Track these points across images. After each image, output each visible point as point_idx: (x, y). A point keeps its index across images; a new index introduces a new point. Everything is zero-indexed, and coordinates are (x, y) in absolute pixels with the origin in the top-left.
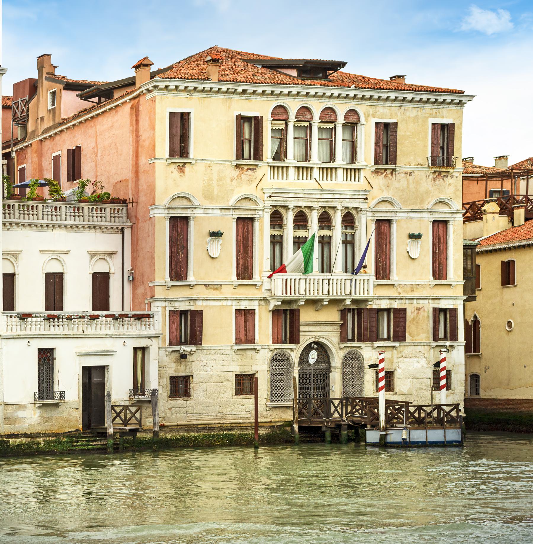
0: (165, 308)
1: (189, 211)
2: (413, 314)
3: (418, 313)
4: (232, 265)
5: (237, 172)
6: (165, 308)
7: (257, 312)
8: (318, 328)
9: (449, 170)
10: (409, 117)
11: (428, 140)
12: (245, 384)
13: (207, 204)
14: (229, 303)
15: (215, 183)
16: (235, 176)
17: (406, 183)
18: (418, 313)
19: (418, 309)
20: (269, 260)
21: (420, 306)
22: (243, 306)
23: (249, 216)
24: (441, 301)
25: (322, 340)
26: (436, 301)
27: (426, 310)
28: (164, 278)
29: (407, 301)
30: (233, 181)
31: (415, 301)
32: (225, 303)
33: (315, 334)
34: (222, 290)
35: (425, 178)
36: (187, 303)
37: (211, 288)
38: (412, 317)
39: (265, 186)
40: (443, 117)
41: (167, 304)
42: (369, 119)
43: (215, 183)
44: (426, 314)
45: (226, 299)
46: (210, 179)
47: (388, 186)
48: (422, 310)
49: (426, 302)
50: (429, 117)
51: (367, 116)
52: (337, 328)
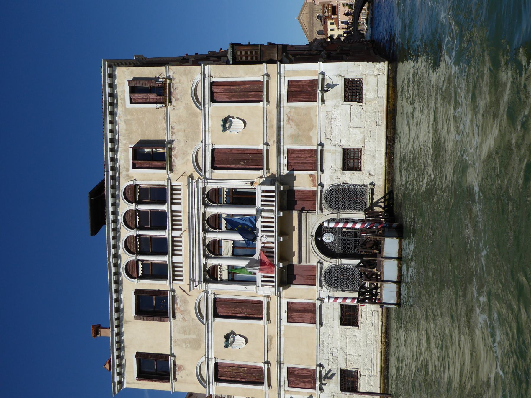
0: (285, 391)
1: (210, 363)
2: (293, 126)
3: (292, 120)
4: (251, 324)
5: (178, 315)
6: (285, 391)
7: (289, 300)
10: (126, 130)
11: (144, 108)
12: (353, 91)
13: (204, 345)
14: (282, 328)
15: (188, 337)
16: (182, 316)
17: (180, 133)
18: (292, 120)
19: (289, 119)
20: (248, 287)
21: (286, 118)
22: (284, 315)
23: (212, 305)
25: (314, 234)
26: (282, 96)
27: (289, 110)
28: (263, 391)
29: (282, 133)
30: (186, 319)
31: (282, 123)
32: (282, 333)
33: (309, 240)
35: (176, 111)
36: (282, 370)
37: (270, 346)
38: (295, 127)
40: (124, 90)
42: (130, 175)
43: (188, 337)
44: (293, 110)
46: (185, 341)
47: (184, 154)
48: (289, 115)
49: (282, 109)
50: (125, 107)
51: (128, 177)
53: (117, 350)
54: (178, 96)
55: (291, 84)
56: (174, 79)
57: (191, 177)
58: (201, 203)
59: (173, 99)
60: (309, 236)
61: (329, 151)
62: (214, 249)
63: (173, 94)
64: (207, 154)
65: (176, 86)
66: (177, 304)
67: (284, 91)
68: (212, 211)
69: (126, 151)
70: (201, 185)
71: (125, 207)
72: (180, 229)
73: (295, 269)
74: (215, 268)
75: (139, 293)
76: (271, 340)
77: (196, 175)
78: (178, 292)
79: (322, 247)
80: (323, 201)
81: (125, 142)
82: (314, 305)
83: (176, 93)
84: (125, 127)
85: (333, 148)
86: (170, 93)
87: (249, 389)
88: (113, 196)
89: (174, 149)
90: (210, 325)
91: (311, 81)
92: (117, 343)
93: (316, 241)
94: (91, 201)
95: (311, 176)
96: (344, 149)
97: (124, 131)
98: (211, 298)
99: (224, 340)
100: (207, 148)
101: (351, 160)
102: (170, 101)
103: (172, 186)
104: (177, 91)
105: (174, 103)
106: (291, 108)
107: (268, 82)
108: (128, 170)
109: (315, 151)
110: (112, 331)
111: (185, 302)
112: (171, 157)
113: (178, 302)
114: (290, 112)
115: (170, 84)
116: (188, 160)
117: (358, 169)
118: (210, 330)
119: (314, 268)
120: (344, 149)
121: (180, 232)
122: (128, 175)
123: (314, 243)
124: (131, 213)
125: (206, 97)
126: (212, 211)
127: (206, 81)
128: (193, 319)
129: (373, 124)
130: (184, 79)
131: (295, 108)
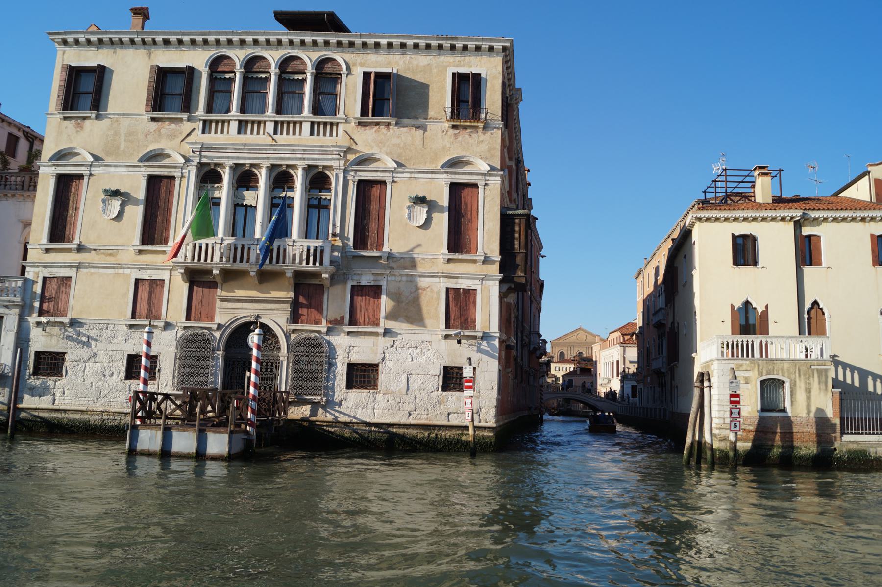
5: (154, 126)
7: (167, 282)
8: (256, 305)
9: (476, 124)
14: (128, 271)
22: (146, 275)
23: (166, 174)
24: (460, 281)
26: (455, 280)
27: (436, 289)
32: (121, 271)
34: (118, 257)
35: (440, 134)
39: (181, 142)
41: (40, 269)
43: (123, 138)
45: (121, 266)
46: (117, 133)
49: (437, 280)
52: (287, 307)
53: (111, 39)
54: (460, 138)
55: (470, 293)
56: (484, 134)
57: (349, 150)
58: (311, 163)
59: (456, 132)
60: (256, 313)
61: (376, 345)
62: (245, 179)
63: (464, 131)
64: (379, 174)
65: (474, 135)
66: (170, 125)
67: (462, 284)
68: (299, 178)
69: (389, 64)
70: (334, 164)
71: (309, 58)
72: (275, 133)
73: (211, 290)
74: (218, 179)
75: (190, 73)
76: (111, 255)
77: (351, 157)
78: (187, 127)
79: (242, 330)
80: (305, 335)
81: (401, 63)
82: (158, 318)
83: (464, 135)
84: (421, 64)
85: (380, 351)
86: (465, 128)
87: (43, 222)
88: (327, 43)
89: (388, 129)
90: (137, 169)
91: (474, 322)
92: (121, 40)
93: (250, 324)
94: (321, 14)
95: (343, 318)
96: (377, 365)
97: (415, 63)
98: (176, 173)
99: (114, 188)
100: (387, 174)
101: (362, 375)
102: (454, 127)
103: (337, 124)
104: (467, 136)
105: (452, 132)
106: (439, 292)
107: (474, 261)
108: (362, 65)
109: (377, 325)
110: (138, 33)
111: (172, 136)
112: (377, 124)
113: (173, 126)
114: (432, 290)
115: (477, 127)
116: (372, 147)
117: (349, 386)
118: (131, 169)
119: (211, 318)
120: (377, 365)
121: (272, 133)
122: (354, 64)
123: (247, 319)
124: (301, 67)
125: (457, 177)
126: (299, 178)
127: (480, 177)
128: (147, 146)
129: (411, 407)
130: (484, 147)
131: (438, 299)
